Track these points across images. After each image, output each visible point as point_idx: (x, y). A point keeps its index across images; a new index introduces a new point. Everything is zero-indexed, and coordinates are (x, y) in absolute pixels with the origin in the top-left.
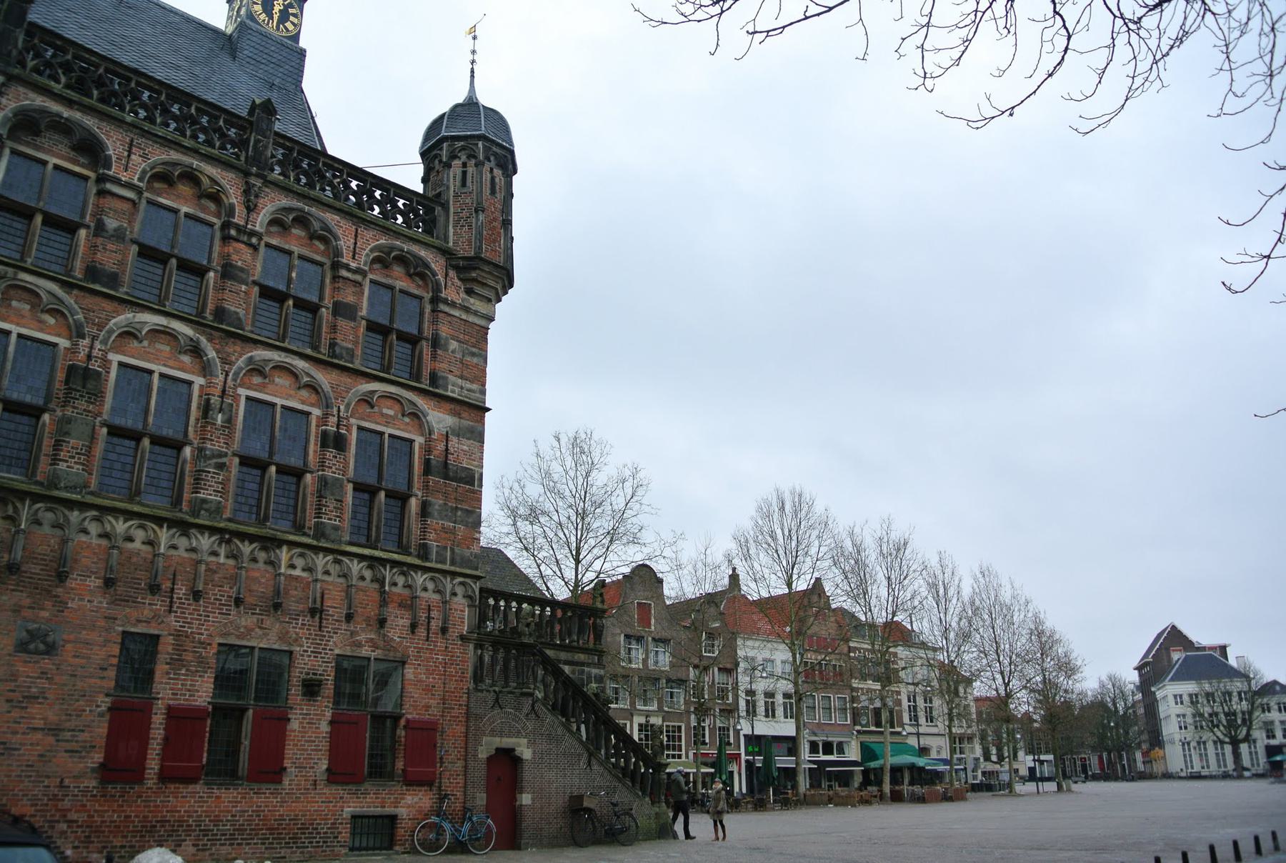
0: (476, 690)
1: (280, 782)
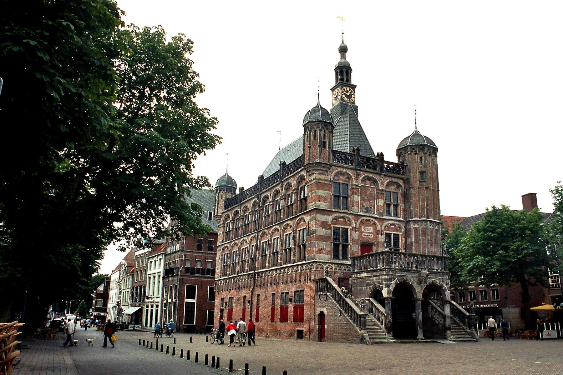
0: (317, 295)
1: (287, 322)
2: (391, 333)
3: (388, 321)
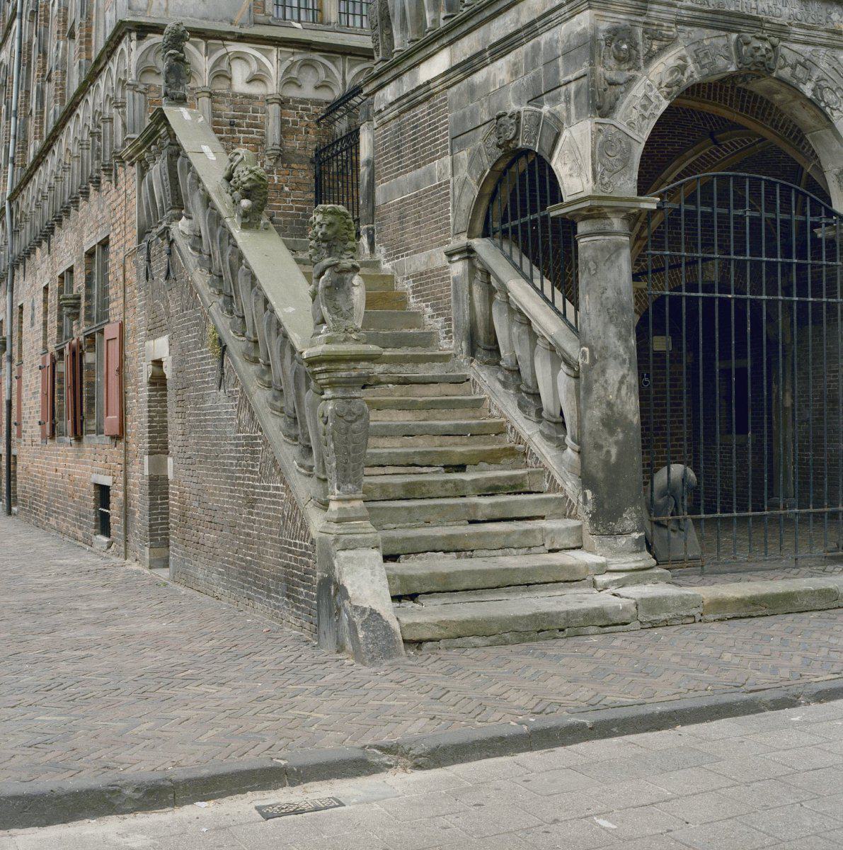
2: (629, 519)
3: (596, 413)
